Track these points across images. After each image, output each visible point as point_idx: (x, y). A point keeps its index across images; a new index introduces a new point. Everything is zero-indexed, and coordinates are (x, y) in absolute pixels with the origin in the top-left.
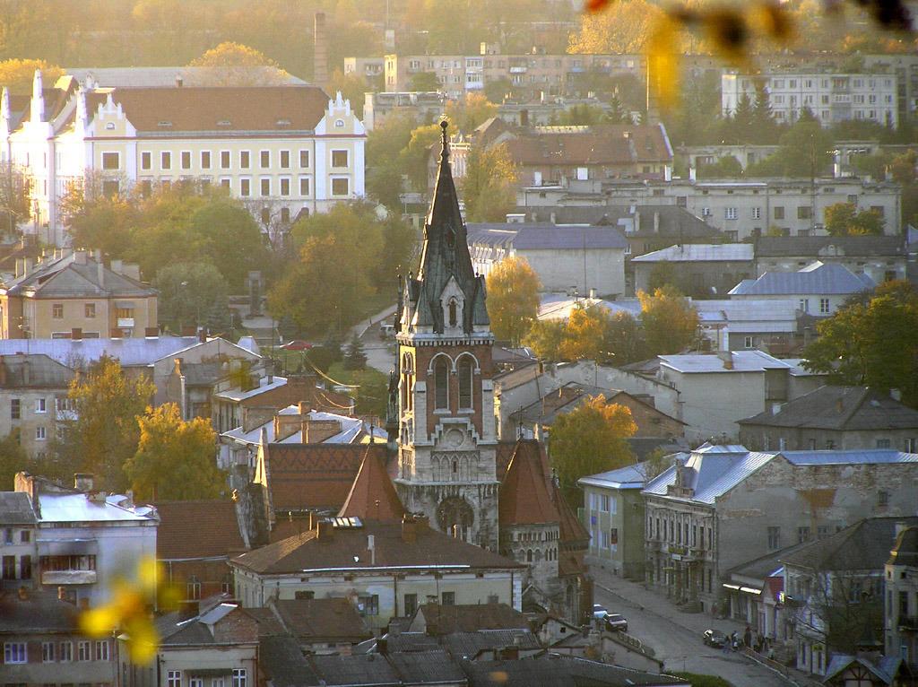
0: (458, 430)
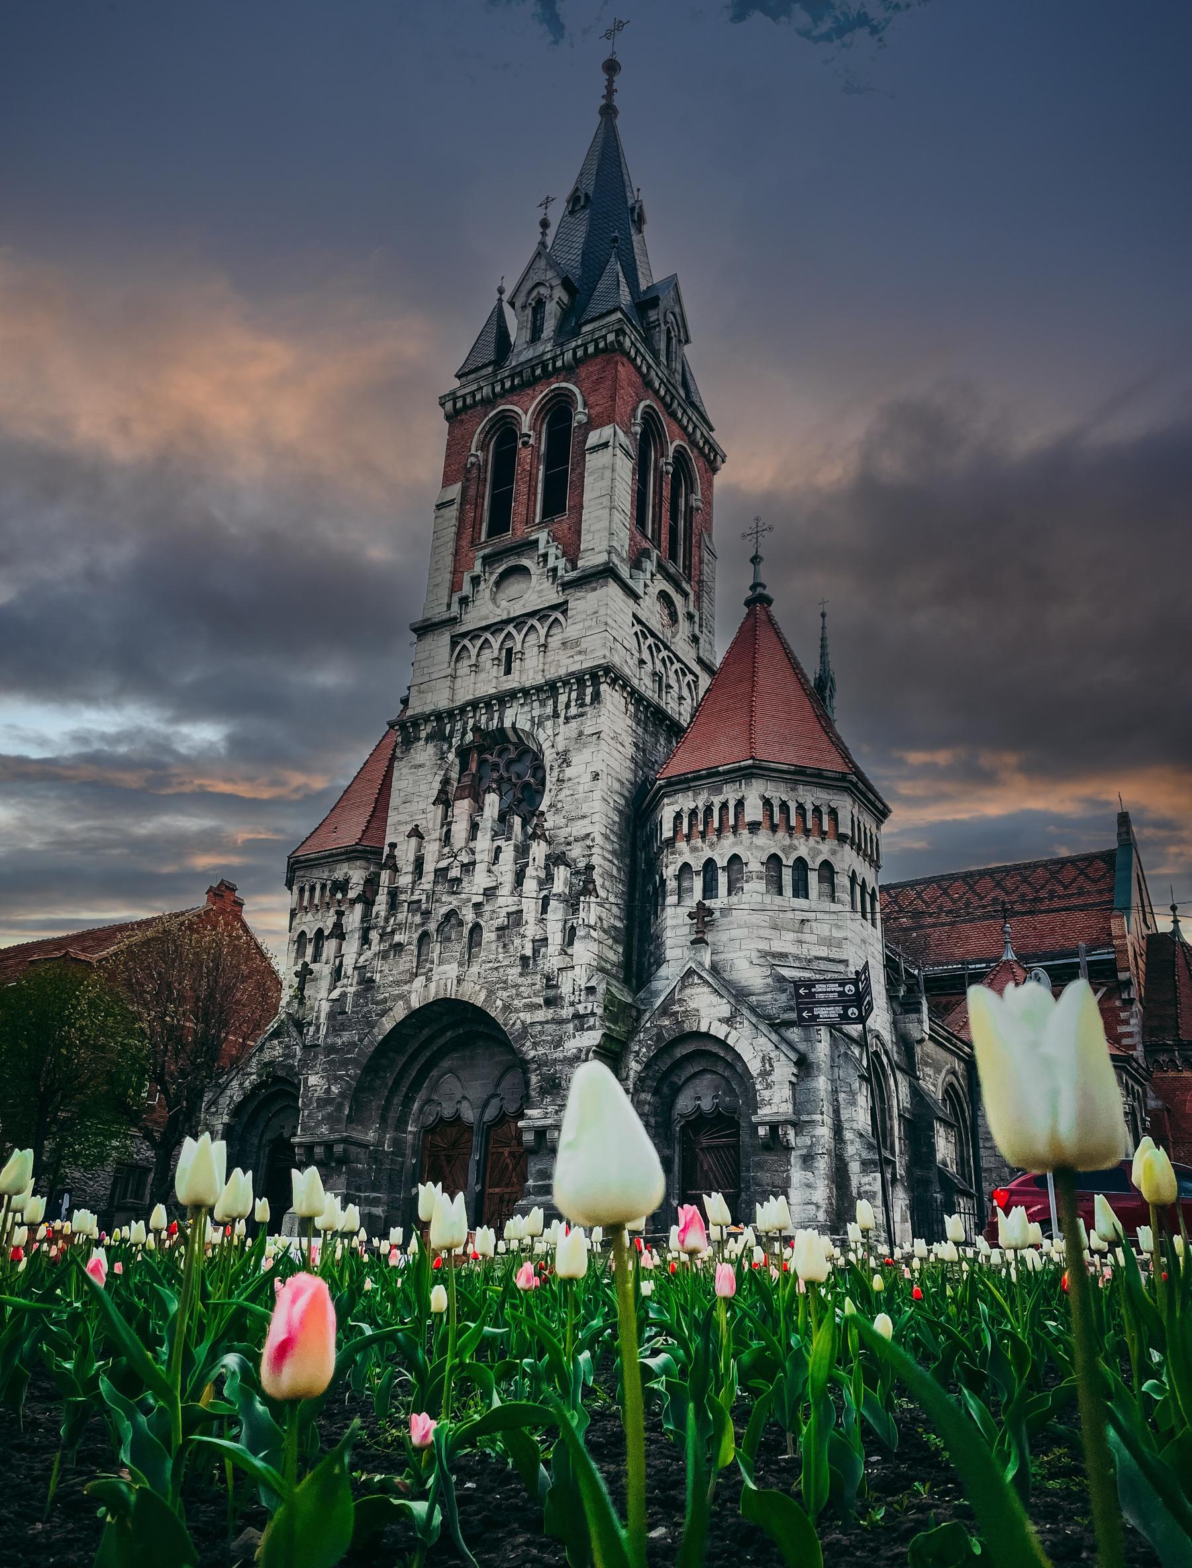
0: (524, 571)
